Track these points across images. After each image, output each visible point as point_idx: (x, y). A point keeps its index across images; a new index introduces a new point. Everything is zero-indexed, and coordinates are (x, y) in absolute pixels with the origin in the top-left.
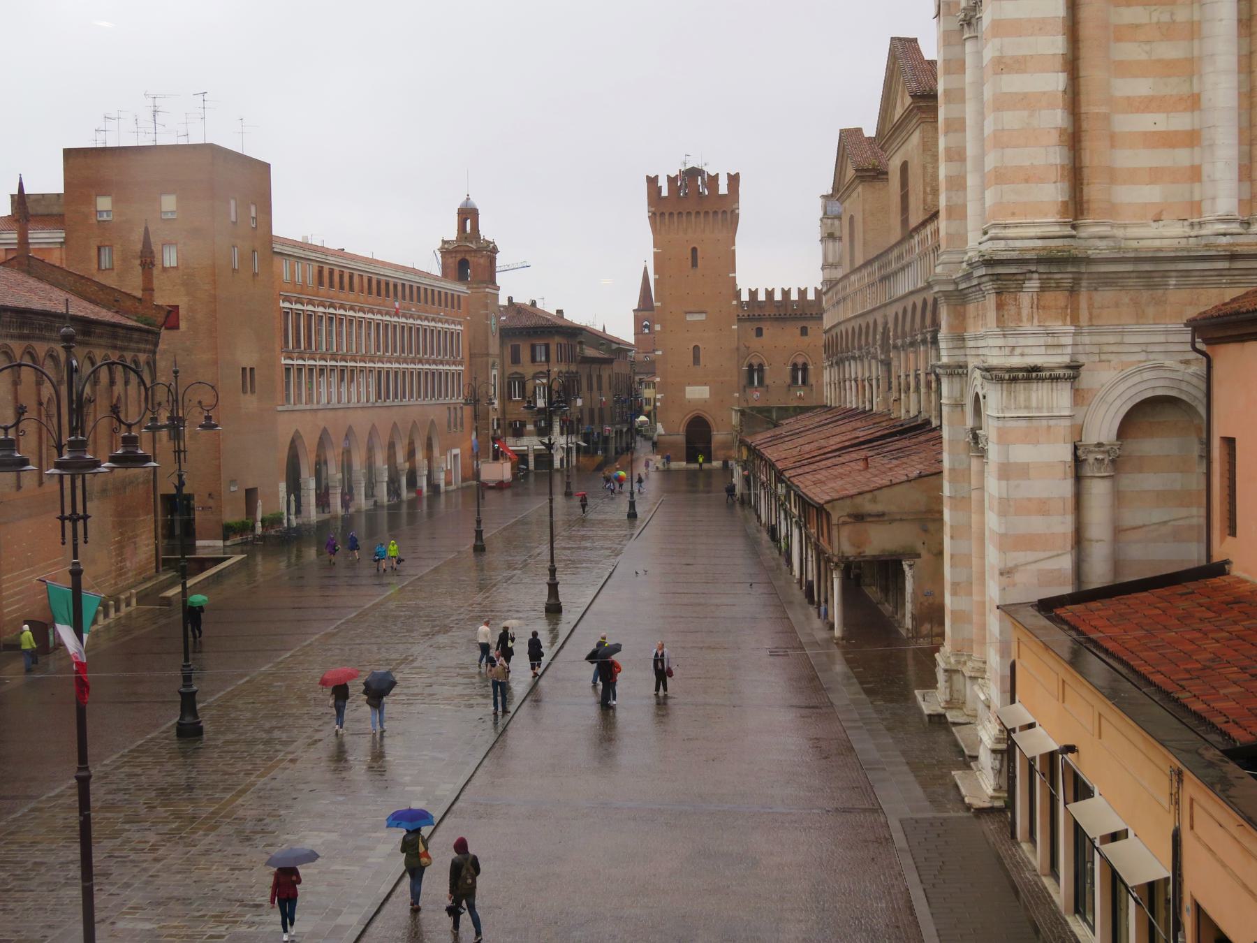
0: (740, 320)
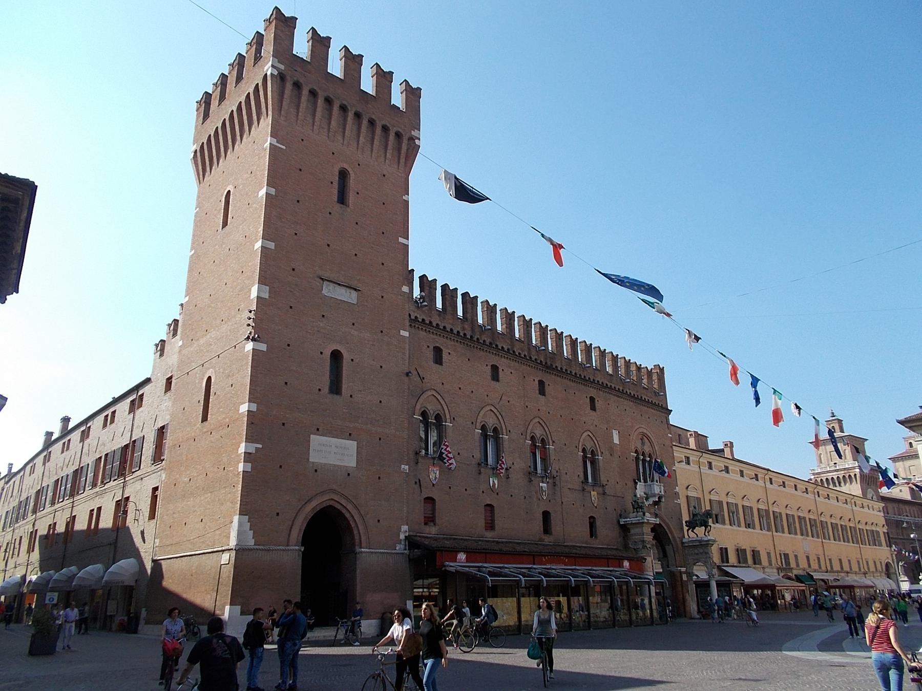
0: (414, 322)
